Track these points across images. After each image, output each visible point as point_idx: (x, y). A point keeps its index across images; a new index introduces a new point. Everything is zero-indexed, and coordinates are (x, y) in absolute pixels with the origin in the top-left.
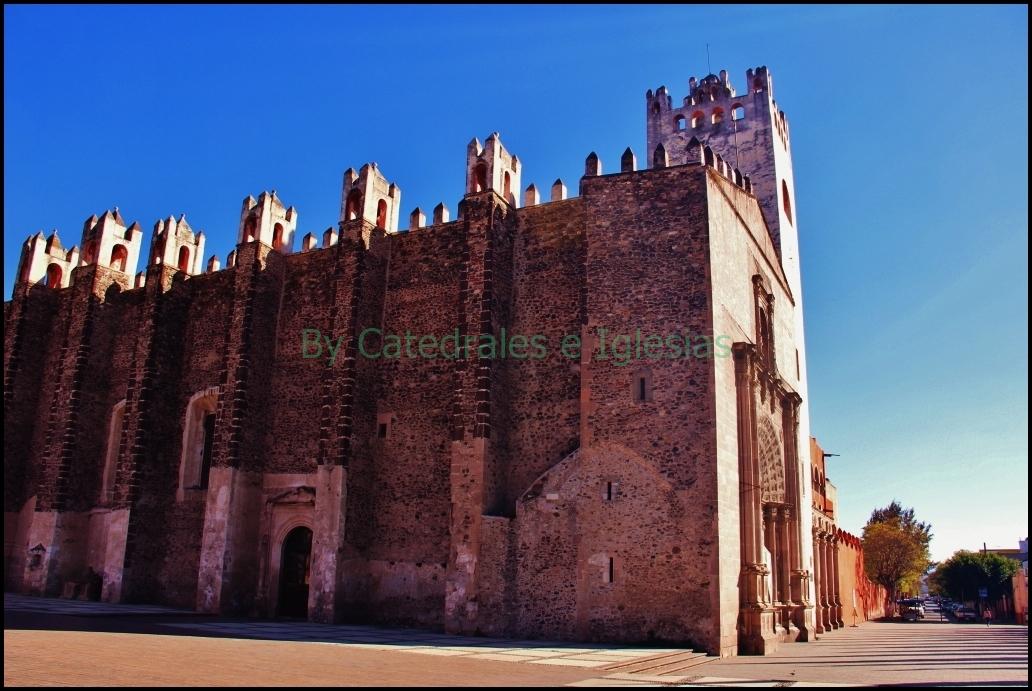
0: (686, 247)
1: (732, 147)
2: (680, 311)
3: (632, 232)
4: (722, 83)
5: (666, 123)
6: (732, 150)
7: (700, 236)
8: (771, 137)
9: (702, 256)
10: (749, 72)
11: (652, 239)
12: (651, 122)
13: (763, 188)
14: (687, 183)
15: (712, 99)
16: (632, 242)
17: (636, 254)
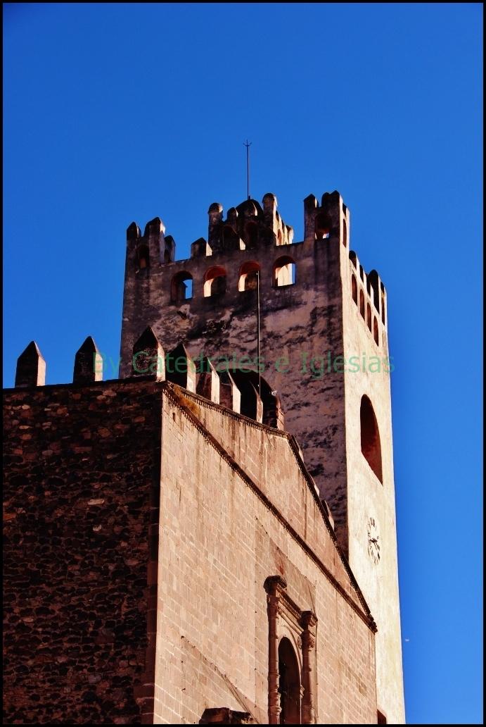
1: (270, 335)
2: (98, 648)
3: (25, 497)
4: (266, 218)
5: (158, 287)
6: (270, 340)
7: (144, 509)
8: (341, 320)
9: (145, 546)
10: (309, 201)
11: (59, 513)
12: (131, 284)
13: (321, 411)
14: (129, 412)
15: (243, 246)
16: (21, 517)
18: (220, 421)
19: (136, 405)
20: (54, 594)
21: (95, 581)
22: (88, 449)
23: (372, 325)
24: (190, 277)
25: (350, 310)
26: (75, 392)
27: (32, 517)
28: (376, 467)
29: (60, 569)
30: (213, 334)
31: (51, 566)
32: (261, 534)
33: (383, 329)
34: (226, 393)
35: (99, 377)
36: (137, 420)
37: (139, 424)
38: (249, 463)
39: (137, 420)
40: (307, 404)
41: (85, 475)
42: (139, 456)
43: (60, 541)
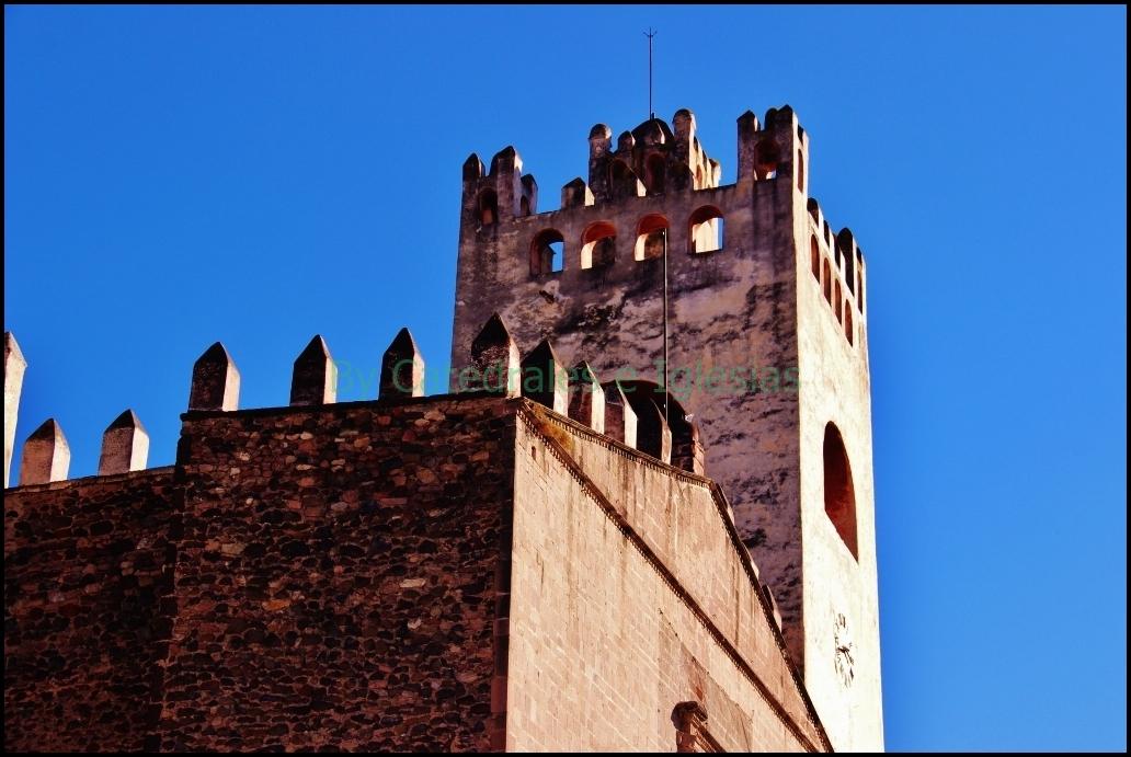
0: (445, 626)
1: (683, 328)
3: (304, 575)
4: (678, 147)
6: (683, 337)
7: (487, 595)
8: (794, 306)
9: (487, 653)
10: (746, 120)
11: (356, 599)
12: (469, 248)
13: (761, 447)
14: (464, 446)
15: (641, 191)
16: (300, 603)
17: (307, 639)
18: (605, 461)
19: (476, 434)
20: (348, 725)
21: (412, 706)
22: (401, 501)
23: (843, 314)
24: (559, 238)
25: (808, 290)
26: (381, 414)
27: (314, 605)
28: (848, 534)
29: (357, 687)
30: (592, 324)
31: (343, 681)
32: (667, 636)
33: (860, 319)
34: (614, 417)
35: (418, 392)
36: (476, 458)
37: (480, 463)
38: (649, 526)
39: (476, 458)
40: (740, 436)
41: (396, 542)
42: (479, 513)
43: (357, 643)
